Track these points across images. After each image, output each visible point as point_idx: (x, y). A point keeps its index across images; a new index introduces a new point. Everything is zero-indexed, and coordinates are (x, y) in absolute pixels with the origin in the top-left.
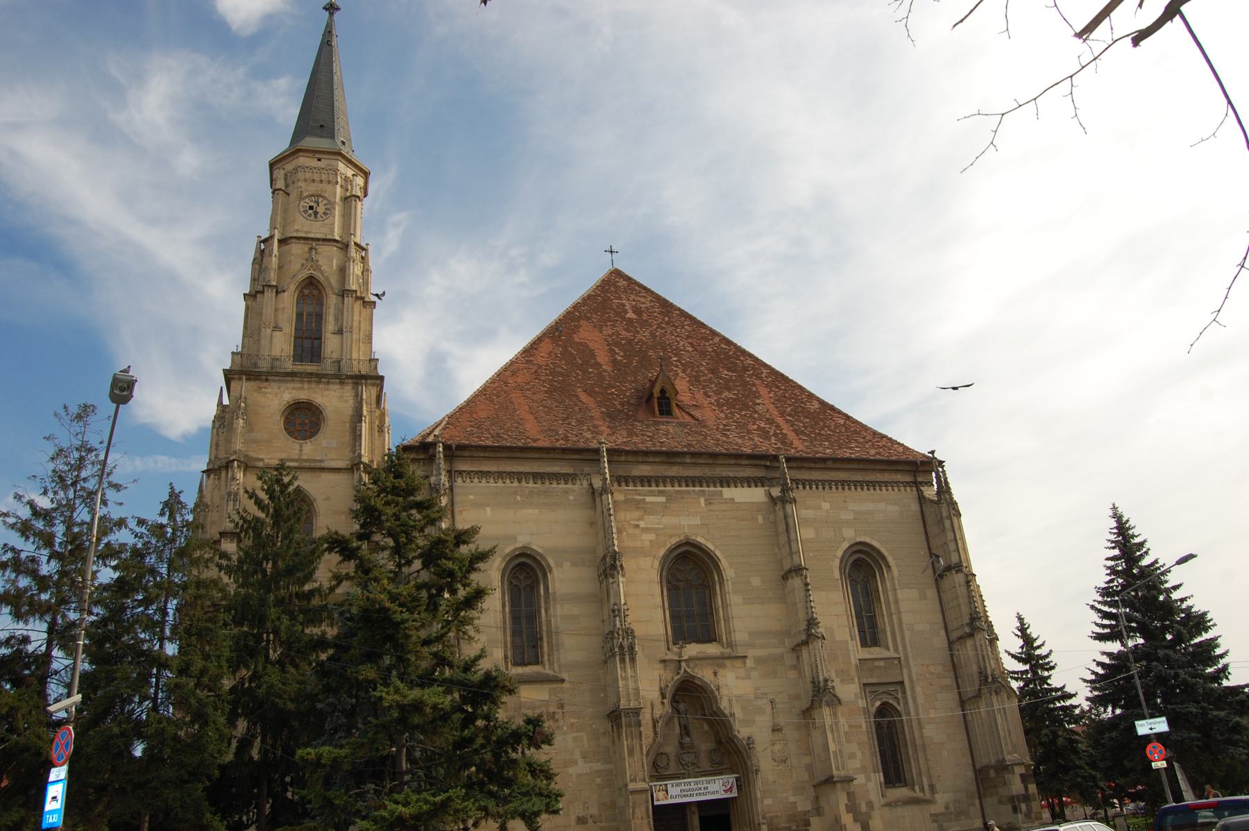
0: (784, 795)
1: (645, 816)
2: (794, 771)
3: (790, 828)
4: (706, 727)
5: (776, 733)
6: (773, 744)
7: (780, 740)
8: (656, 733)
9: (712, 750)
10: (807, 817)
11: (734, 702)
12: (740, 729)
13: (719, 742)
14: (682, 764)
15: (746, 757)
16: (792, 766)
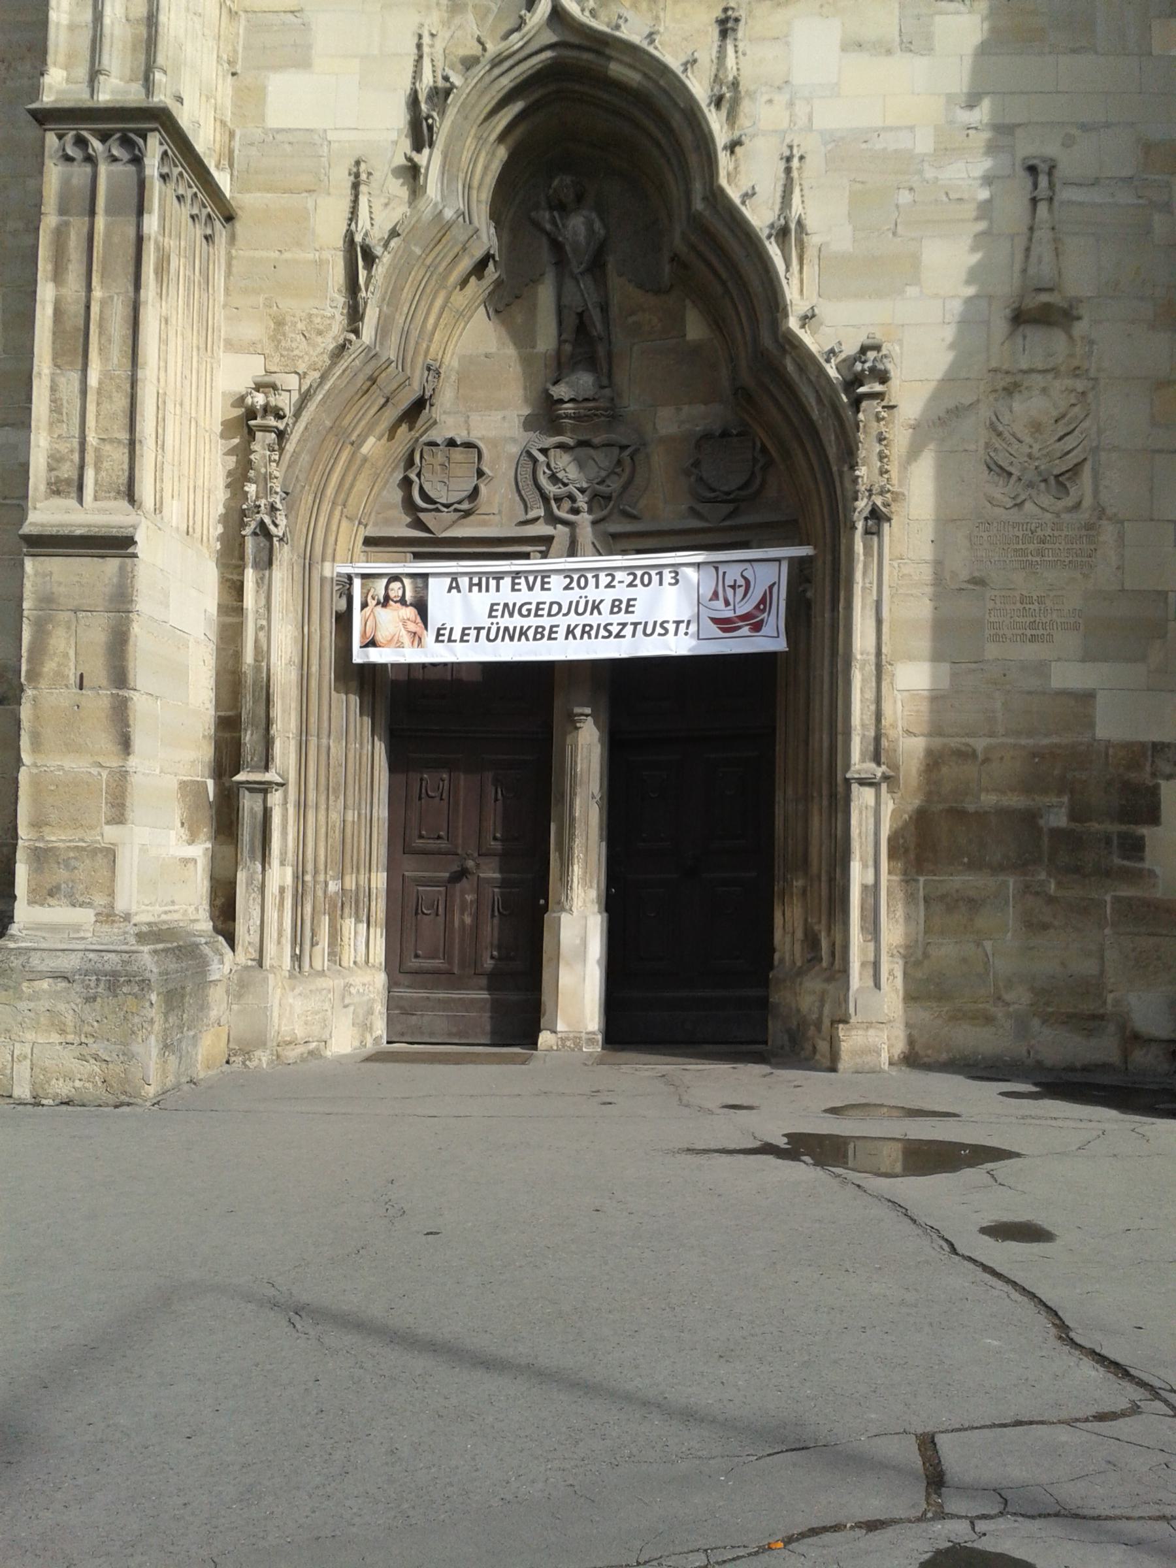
0: (1030, 652)
1: (97, 671)
2: (1108, 533)
3: (1030, 818)
4: (695, 329)
5: (1035, 335)
6: (1010, 390)
7: (1054, 371)
8: (355, 315)
9: (707, 436)
10: (1144, 776)
11: (809, 174)
12: (827, 310)
13: (743, 396)
14: (545, 498)
15: (832, 451)
16: (1100, 511)
